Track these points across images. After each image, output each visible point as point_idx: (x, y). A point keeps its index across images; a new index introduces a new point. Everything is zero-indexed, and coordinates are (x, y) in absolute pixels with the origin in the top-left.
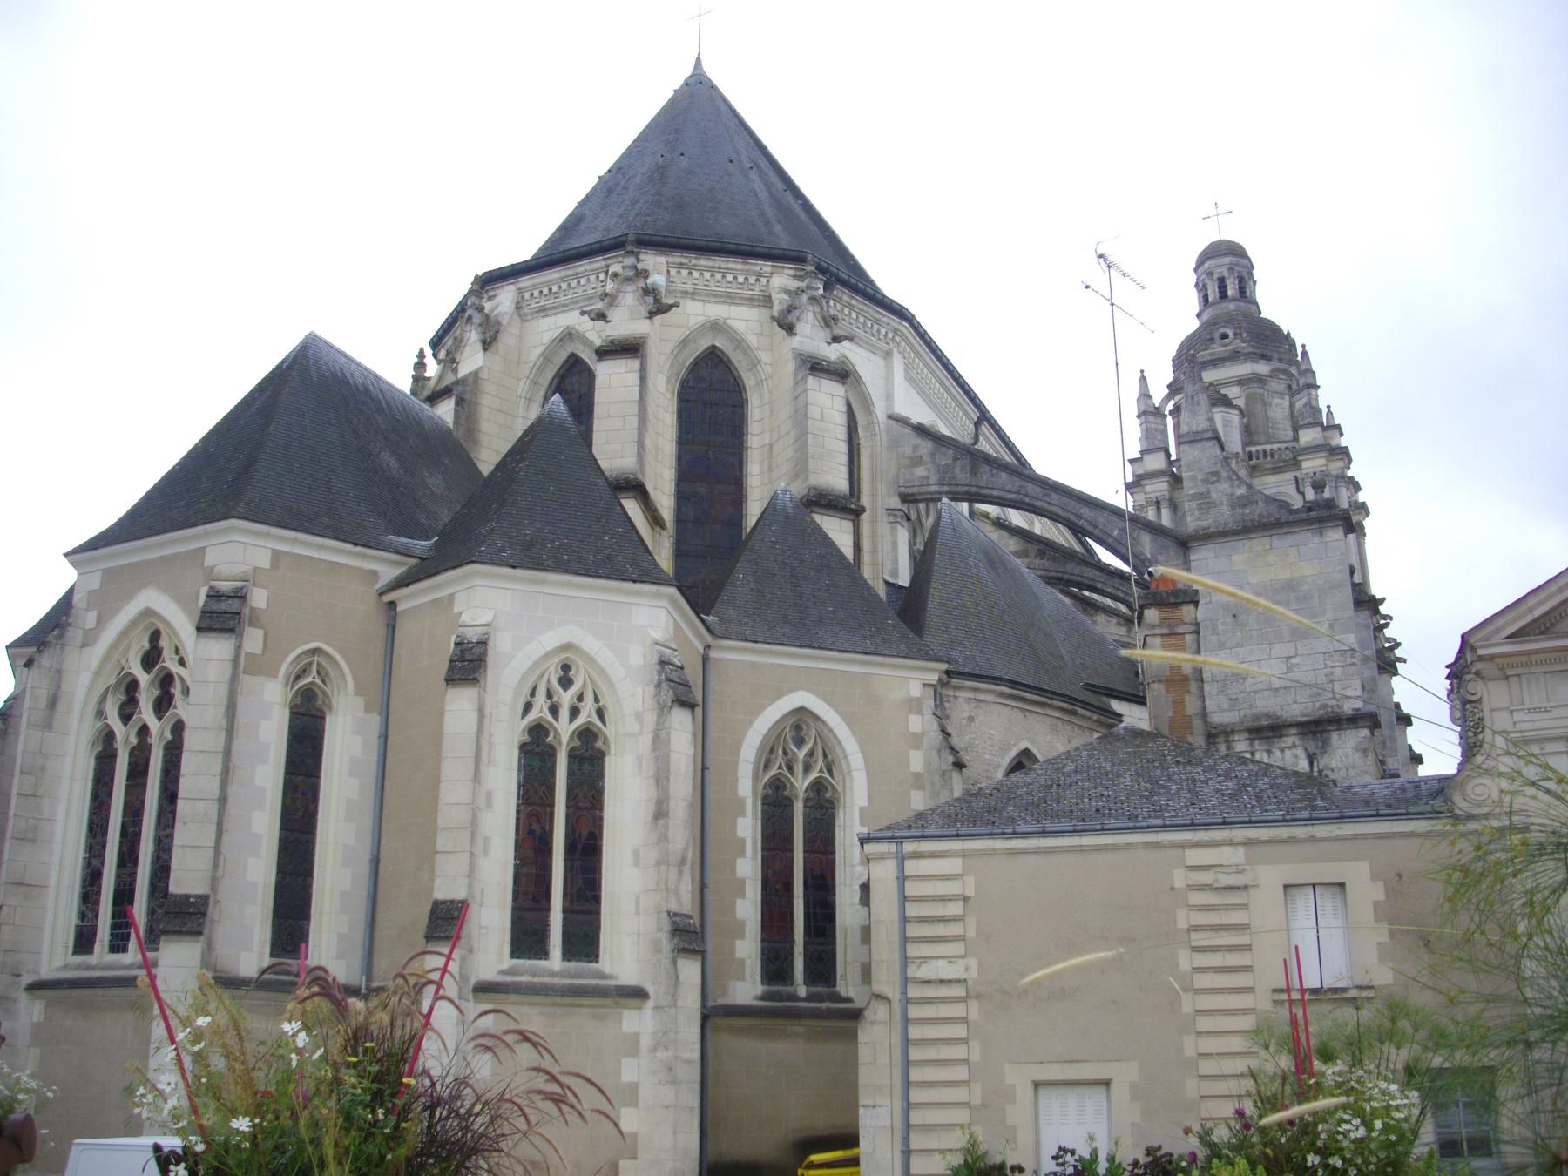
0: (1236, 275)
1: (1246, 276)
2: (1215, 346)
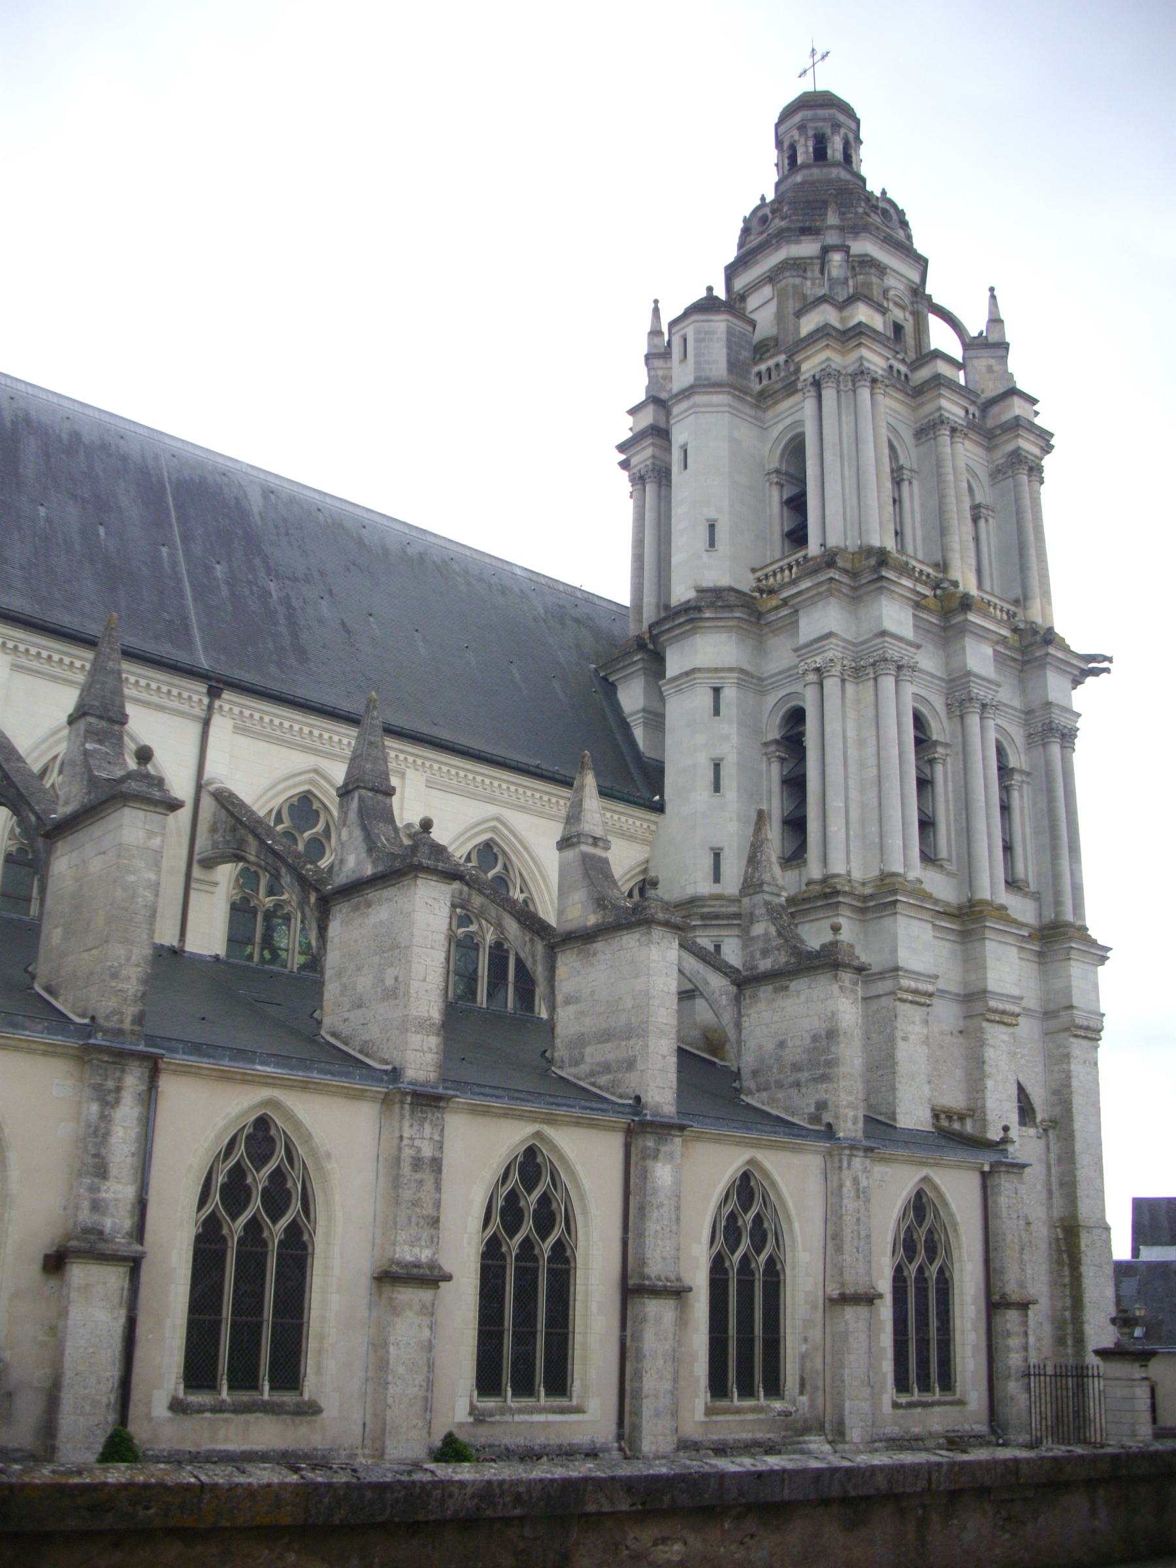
0: (811, 133)
1: (828, 131)
2: (752, 237)
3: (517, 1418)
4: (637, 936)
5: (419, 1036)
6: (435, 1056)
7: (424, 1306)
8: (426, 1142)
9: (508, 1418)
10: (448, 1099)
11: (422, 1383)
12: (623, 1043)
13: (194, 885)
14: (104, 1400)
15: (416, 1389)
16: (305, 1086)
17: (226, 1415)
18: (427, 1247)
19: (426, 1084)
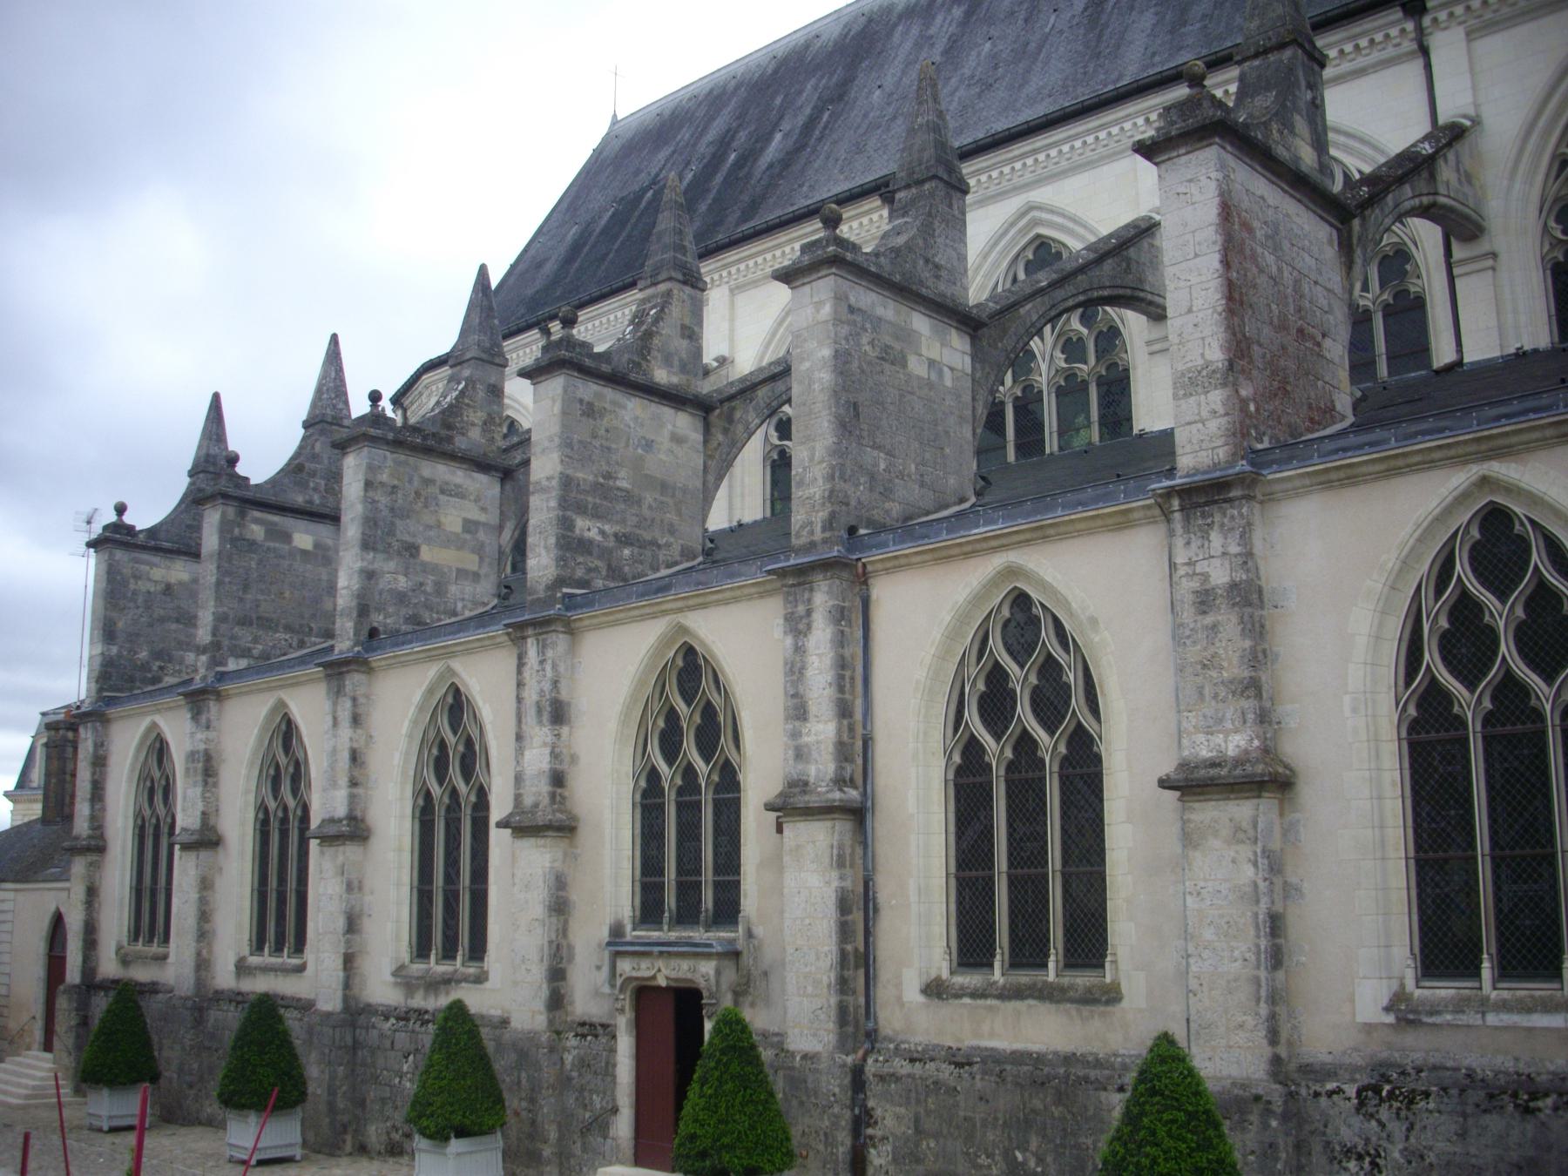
3: (1492, 1019)
5: (1192, 400)
6: (1224, 420)
7: (1238, 829)
8: (1217, 562)
9: (1472, 1018)
11: (1247, 955)
13: (1456, 271)
14: (825, 980)
15: (1238, 964)
16: (1041, 535)
17: (989, 1002)
18: (1236, 731)
19: (1216, 466)
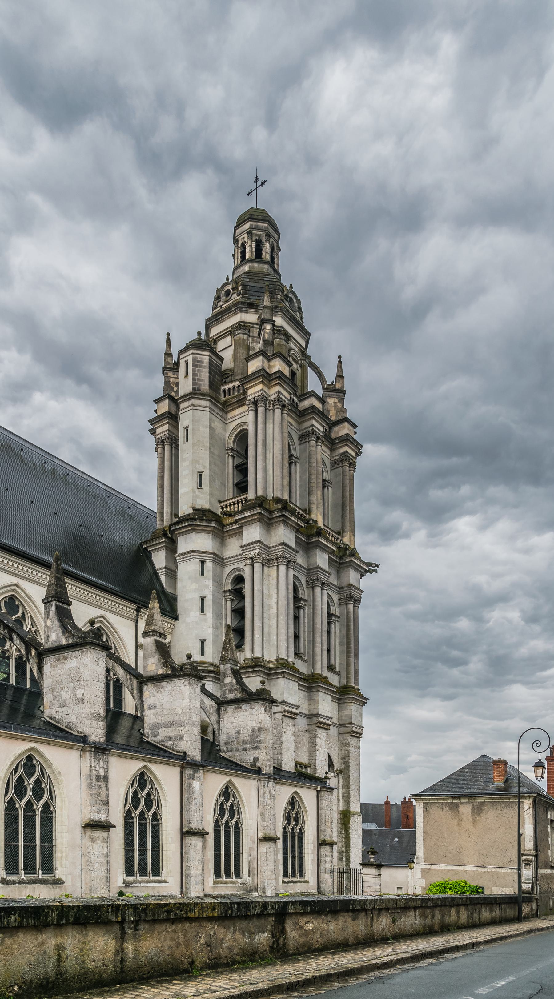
4: (183, 681)
8: (101, 769)
10: (109, 751)
12: (177, 728)
17: (25, 885)
